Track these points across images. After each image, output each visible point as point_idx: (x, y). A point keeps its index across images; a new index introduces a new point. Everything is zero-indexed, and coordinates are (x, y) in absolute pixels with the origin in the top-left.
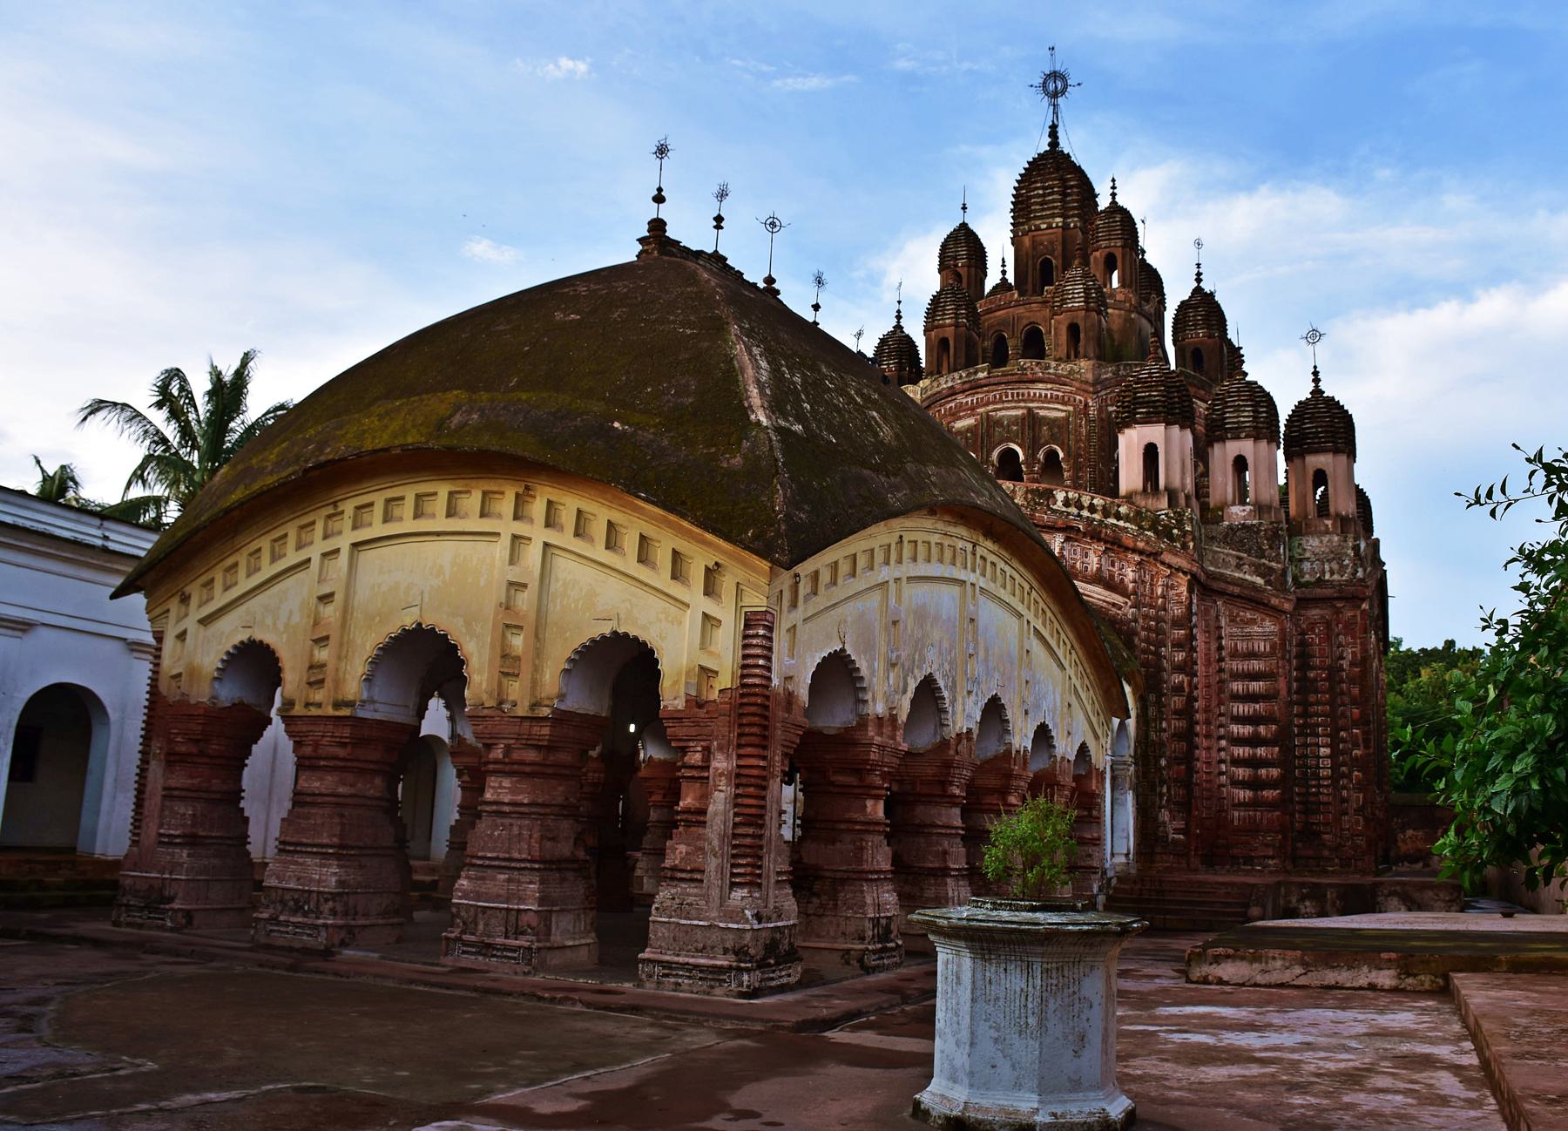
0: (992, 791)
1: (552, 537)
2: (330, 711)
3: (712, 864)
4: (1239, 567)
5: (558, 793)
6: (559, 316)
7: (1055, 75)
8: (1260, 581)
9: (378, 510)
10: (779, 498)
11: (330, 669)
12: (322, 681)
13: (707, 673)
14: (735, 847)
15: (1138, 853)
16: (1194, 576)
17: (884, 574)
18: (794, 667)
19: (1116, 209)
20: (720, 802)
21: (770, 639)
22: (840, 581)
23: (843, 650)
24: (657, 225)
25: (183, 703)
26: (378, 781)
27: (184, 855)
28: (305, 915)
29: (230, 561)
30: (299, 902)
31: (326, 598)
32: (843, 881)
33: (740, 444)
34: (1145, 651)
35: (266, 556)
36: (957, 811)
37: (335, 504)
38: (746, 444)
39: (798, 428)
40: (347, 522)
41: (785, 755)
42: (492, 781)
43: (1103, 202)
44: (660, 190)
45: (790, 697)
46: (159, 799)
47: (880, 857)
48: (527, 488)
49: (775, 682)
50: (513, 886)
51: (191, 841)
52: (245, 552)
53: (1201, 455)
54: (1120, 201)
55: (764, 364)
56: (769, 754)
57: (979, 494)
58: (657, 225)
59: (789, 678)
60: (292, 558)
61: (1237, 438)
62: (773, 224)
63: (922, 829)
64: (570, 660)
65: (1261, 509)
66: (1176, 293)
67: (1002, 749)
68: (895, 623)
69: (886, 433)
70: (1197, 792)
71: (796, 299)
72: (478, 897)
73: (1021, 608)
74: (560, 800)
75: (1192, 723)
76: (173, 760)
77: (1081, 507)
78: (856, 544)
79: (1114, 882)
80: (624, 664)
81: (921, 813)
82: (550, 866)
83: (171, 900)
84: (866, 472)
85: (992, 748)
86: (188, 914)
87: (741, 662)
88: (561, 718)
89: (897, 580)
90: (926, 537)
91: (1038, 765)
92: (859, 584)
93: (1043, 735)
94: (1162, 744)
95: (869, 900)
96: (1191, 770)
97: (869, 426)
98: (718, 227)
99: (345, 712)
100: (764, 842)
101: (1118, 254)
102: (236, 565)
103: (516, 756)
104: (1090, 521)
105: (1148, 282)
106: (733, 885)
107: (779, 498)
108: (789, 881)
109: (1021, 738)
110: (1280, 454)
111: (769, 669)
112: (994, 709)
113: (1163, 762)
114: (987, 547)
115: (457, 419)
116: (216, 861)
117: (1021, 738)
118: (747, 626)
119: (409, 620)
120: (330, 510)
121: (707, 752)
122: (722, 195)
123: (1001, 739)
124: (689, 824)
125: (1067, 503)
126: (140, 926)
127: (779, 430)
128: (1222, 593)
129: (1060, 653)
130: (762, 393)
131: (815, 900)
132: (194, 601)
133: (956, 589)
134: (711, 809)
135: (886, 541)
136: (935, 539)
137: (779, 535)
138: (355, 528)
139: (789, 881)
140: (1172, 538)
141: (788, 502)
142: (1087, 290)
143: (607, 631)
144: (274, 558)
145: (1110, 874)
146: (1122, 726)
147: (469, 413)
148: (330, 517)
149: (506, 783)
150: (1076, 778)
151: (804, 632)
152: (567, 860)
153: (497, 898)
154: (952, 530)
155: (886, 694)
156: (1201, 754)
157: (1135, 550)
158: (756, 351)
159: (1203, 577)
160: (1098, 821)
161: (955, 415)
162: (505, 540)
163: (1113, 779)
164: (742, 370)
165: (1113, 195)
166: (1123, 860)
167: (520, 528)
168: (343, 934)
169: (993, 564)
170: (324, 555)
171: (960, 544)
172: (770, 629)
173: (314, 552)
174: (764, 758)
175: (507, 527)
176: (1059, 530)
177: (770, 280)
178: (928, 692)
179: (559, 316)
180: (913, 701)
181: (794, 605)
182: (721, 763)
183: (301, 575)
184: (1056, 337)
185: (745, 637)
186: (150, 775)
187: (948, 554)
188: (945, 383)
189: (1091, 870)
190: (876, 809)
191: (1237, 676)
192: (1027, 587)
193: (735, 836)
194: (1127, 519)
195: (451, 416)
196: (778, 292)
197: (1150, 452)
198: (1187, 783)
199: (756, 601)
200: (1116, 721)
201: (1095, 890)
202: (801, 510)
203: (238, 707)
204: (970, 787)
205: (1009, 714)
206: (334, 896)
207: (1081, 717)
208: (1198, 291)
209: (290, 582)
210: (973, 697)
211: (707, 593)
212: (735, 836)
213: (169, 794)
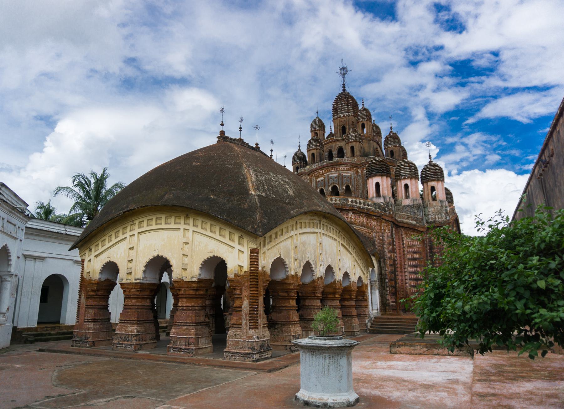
0: (331, 294)
1: (195, 229)
2: (134, 281)
3: (244, 322)
4: (408, 218)
5: (200, 302)
6: (194, 164)
7: (343, 68)
8: (414, 222)
9: (145, 222)
10: (258, 216)
11: (133, 269)
12: (131, 273)
13: (241, 267)
14: (250, 317)
15: (381, 309)
16: (393, 222)
17: (292, 233)
18: (265, 262)
19: (364, 109)
20: (246, 305)
21: (258, 256)
22: (278, 237)
23: (280, 257)
24: (222, 133)
25: (90, 280)
26: (148, 300)
27: (92, 325)
28: (128, 341)
29: (103, 239)
30: (125, 337)
31: (131, 249)
32: (284, 324)
33: (246, 201)
34: (379, 247)
35: (113, 237)
36: (319, 301)
37: (133, 221)
38: (248, 200)
39: (263, 194)
40: (136, 227)
41: (264, 289)
42: (180, 300)
43: (360, 107)
44: (222, 122)
45: (264, 273)
46: (84, 309)
47: (295, 316)
48: (187, 215)
49: (260, 268)
50: (187, 331)
51: (94, 321)
52: (108, 236)
53: (394, 185)
54: (366, 106)
55: (253, 175)
56: (259, 289)
57: (320, 207)
58: (222, 133)
59: (264, 267)
60: (121, 237)
61: (405, 179)
62: (257, 128)
63: (309, 308)
64: (202, 264)
65: (413, 200)
66: (384, 133)
67: (333, 281)
68: (296, 247)
69: (291, 192)
70: (398, 289)
71: (266, 149)
72: (177, 334)
73: (336, 238)
74: (201, 305)
75: (395, 268)
76: (88, 297)
77: (357, 203)
78: (284, 226)
79: (373, 319)
80: (217, 265)
81: (307, 303)
82: (197, 324)
83: (88, 338)
84: (284, 205)
85: (330, 280)
86: (93, 342)
87: (249, 263)
88: (200, 281)
89: (296, 234)
90: (304, 221)
91: (346, 284)
92: (285, 237)
93: (346, 275)
94: (386, 275)
95: (292, 330)
96: (395, 282)
97: (285, 191)
98: (240, 131)
99: (138, 281)
100: (258, 315)
101: (365, 123)
102: (105, 240)
103: (187, 292)
104: (359, 208)
105: (377, 131)
106: (250, 328)
107: (258, 216)
108: (267, 326)
109: (339, 276)
110: (419, 182)
111: (258, 265)
112: (329, 269)
113: (387, 281)
114: (324, 221)
115: (166, 196)
116: (102, 326)
117: (339, 276)
118: (251, 253)
119: (155, 255)
120: (131, 223)
121: (241, 289)
122: (241, 121)
123: (332, 277)
124: (237, 311)
125: (352, 202)
126: (79, 347)
127: (259, 196)
128: (403, 227)
129: (350, 250)
130: (253, 185)
131: (276, 330)
132: (93, 250)
133: (315, 235)
134: (243, 306)
135: (292, 224)
136: (307, 221)
137: (258, 226)
138: (139, 228)
139: (267, 326)
140: (385, 211)
141: (261, 217)
142: (356, 135)
143: (212, 256)
144: (116, 237)
145: (372, 316)
146: (373, 270)
147: (170, 194)
148: (131, 225)
149: (185, 300)
150: (358, 287)
151: (268, 253)
152: (203, 322)
153: (183, 334)
154: (313, 218)
155: (294, 268)
156: (399, 277)
157: (374, 216)
158: (251, 172)
159: (396, 223)
160: (366, 300)
161: (317, 177)
162: (182, 230)
163: (371, 286)
164: (247, 178)
165: (363, 105)
166: (376, 311)
167: (186, 227)
168: (139, 346)
169: (327, 226)
170: (130, 236)
171: (315, 222)
172: (258, 253)
173: (127, 235)
174: (257, 291)
175: (182, 226)
176: (350, 210)
177: (257, 144)
178: (308, 267)
179: (194, 164)
180: (303, 270)
181: (264, 246)
182: (245, 293)
183: (124, 242)
184: (347, 151)
185: (251, 256)
186: (82, 302)
187: (312, 225)
188: (315, 166)
189: (366, 315)
190: (293, 303)
191: (409, 253)
192: (338, 231)
193: (250, 314)
194: (371, 206)
195: (164, 195)
196: (259, 148)
197: (377, 185)
198: (395, 287)
199: (253, 246)
200: (370, 269)
201: (367, 322)
202: (265, 219)
203: (107, 280)
204: (323, 293)
205: (334, 270)
206: (136, 335)
207: (359, 268)
208: (391, 132)
209: (120, 244)
210: (322, 266)
211: (239, 244)
212: (250, 314)
213: (88, 307)
